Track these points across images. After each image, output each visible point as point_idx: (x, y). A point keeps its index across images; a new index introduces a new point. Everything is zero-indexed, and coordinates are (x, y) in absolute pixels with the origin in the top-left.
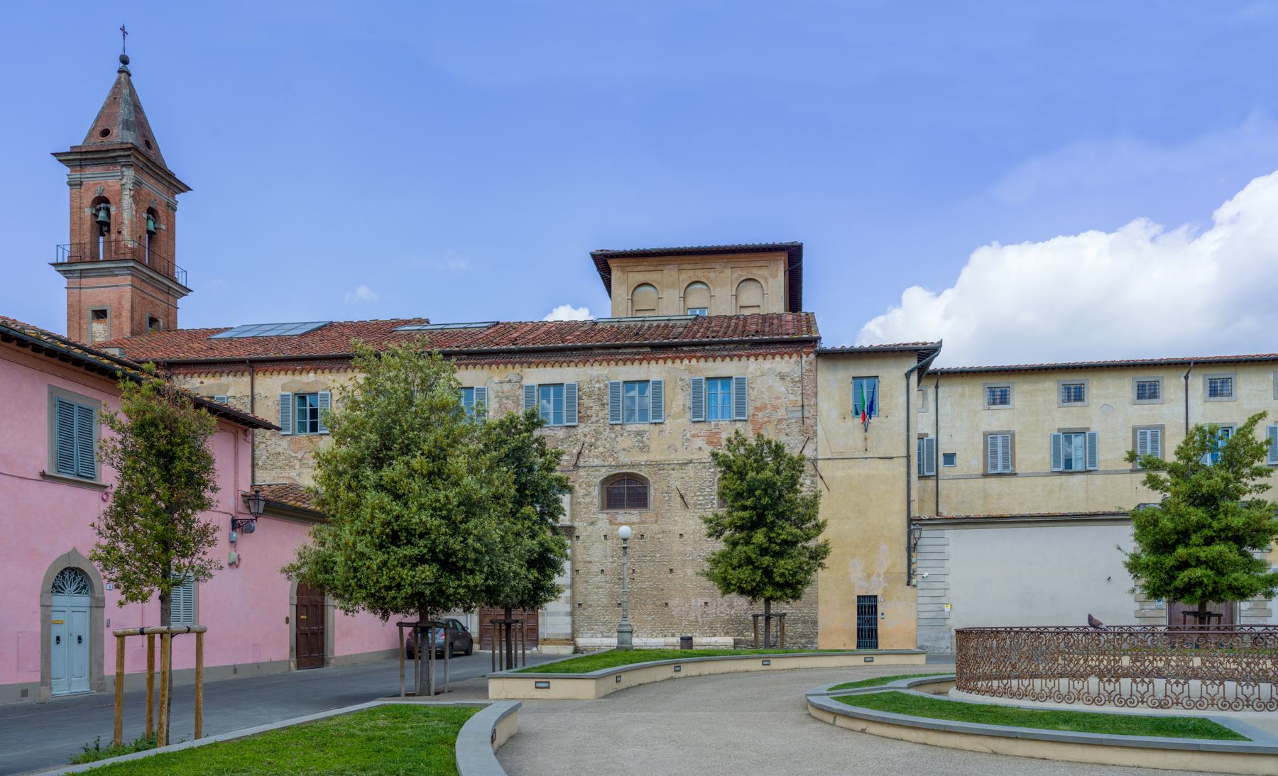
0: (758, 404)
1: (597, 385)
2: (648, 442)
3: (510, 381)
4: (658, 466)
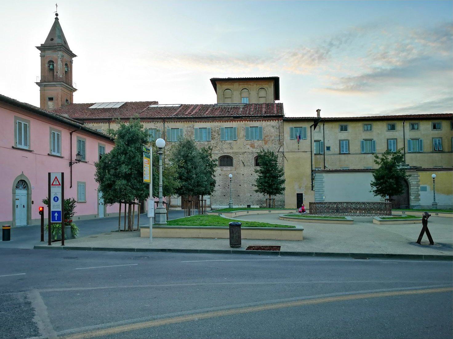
0: (266, 135)
1: (217, 129)
3: (190, 127)
4: (236, 153)
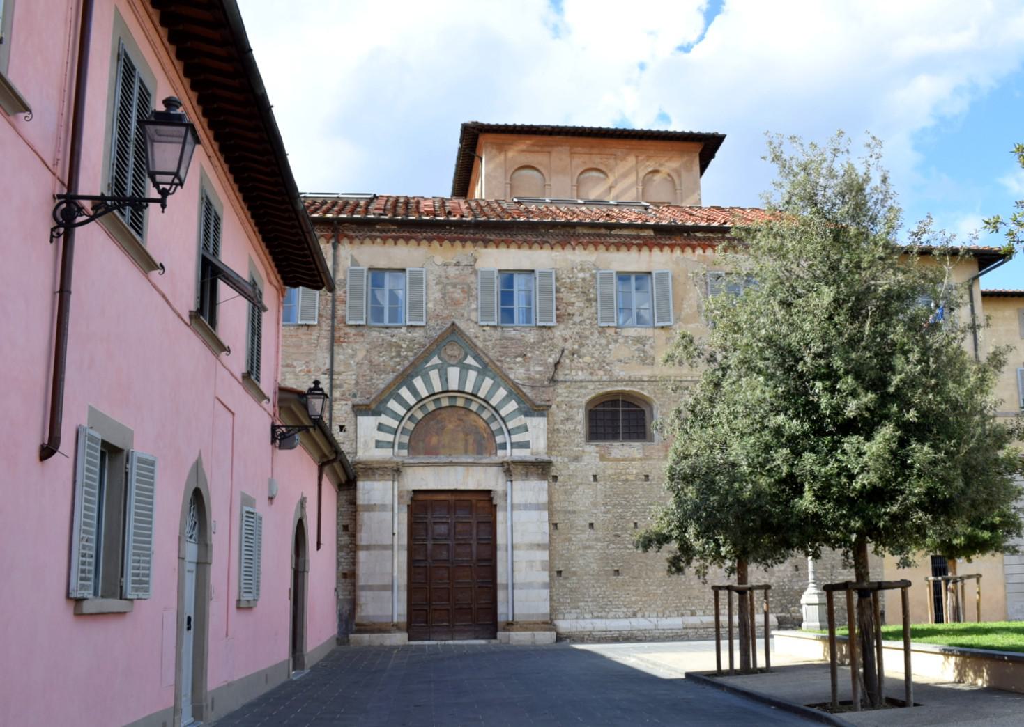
1: (581, 275)
2: (651, 352)
3: (458, 264)
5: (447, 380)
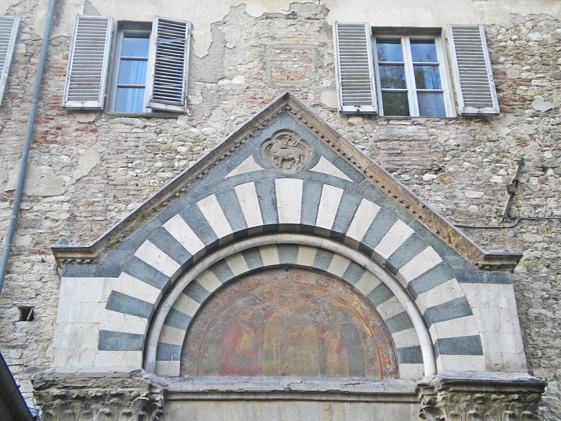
5: (274, 203)
